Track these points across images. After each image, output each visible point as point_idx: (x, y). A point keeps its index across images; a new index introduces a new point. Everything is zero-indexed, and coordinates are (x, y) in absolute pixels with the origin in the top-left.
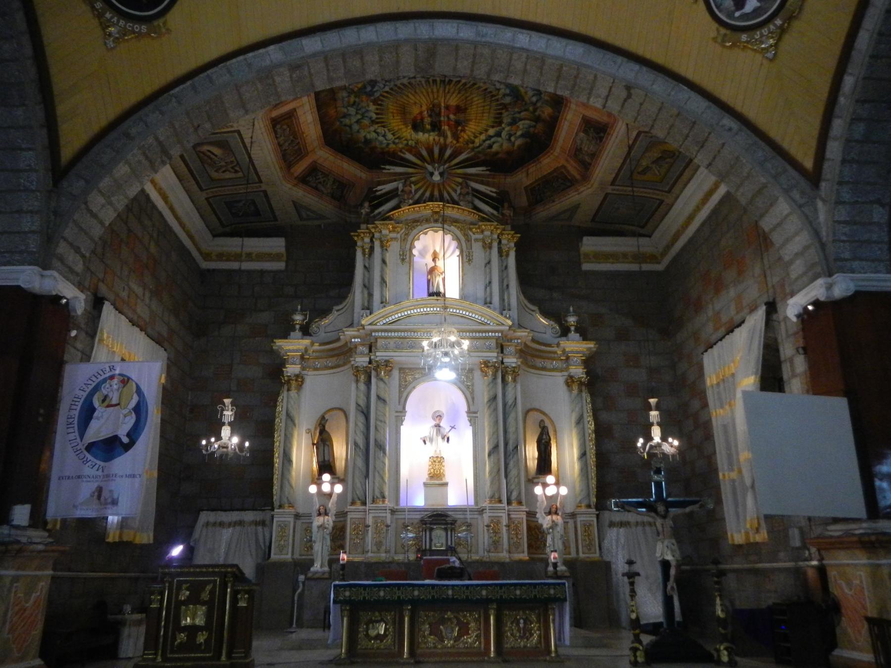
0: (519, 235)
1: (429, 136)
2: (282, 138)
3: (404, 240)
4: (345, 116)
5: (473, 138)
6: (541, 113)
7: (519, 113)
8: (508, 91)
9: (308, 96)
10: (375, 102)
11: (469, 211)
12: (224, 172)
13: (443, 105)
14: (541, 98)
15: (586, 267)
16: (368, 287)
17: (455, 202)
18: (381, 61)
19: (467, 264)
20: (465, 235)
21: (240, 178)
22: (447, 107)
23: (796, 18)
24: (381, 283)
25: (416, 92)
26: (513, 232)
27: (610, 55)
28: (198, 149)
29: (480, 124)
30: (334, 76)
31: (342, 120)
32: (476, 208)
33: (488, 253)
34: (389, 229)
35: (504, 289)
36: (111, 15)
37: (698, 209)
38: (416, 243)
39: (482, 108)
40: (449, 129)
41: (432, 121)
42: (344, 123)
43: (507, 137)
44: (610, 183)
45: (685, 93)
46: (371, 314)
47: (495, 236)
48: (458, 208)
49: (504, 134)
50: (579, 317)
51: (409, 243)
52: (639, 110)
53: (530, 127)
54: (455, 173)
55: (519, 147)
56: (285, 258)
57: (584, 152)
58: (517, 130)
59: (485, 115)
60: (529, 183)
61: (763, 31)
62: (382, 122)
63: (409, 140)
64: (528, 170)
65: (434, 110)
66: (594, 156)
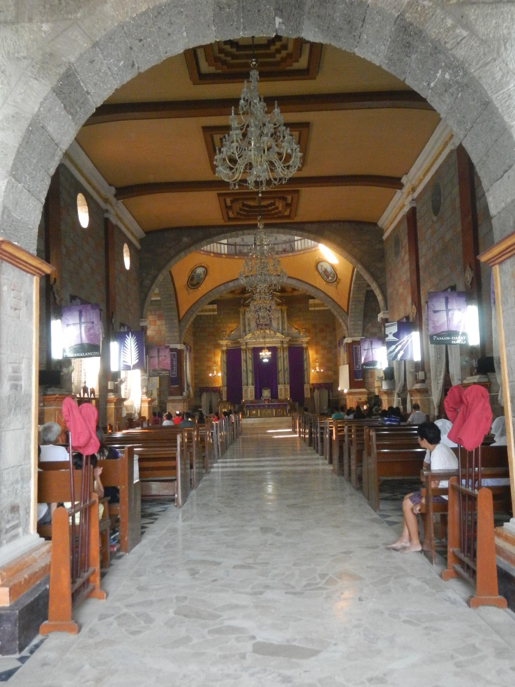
15: (310, 309)
16: (244, 325)
35: (283, 324)
46: (246, 335)
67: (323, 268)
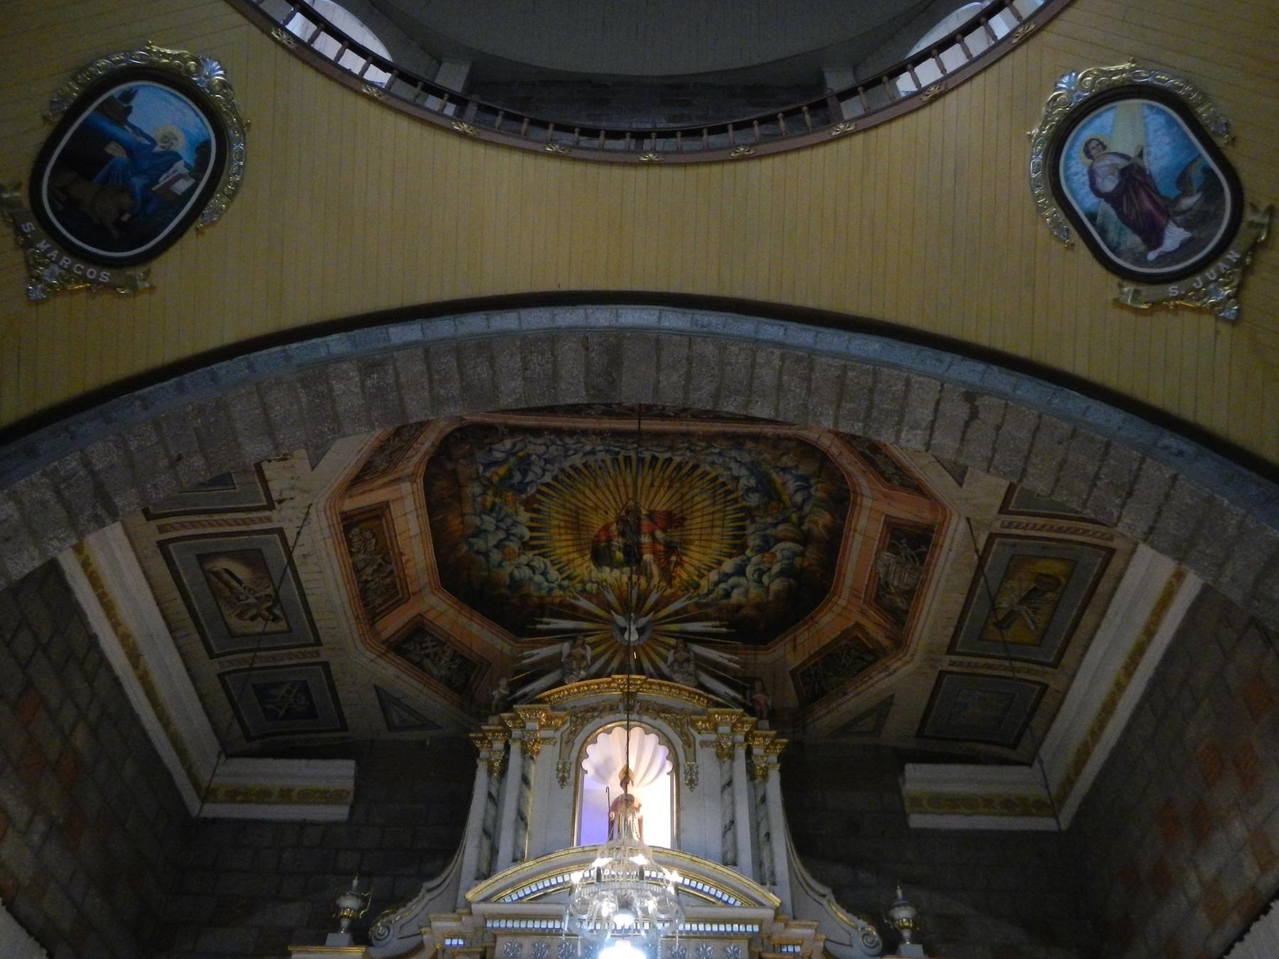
0: (785, 741)
1: (622, 573)
2: (361, 556)
3: (566, 743)
4: (480, 532)
5: (696, 579)
6: (813, 526)
7: (775, 525)
8: (753, 482)
9: (412, 483)
10: (529, 505)
11: (690, 692)
12: (253, 618)
13: (644, 512)
14: (809, 493)
16: (491, 834)
17: (662, 676)
18: (526, 369)
19: (685, 790)
20: (683, 734)
21: (282, 632)
22: (651, 515)
23: (1264, 245)
24: (516, 821)
25: (597, 485)
26: (773, 733)
27: (928, 352)
28: (208, 566)
29: (708, 551)
30: (442, 392)
31: (474, 540)
32: (701, 686)
33: (726, 766)
34: (540, 720)
35: (761, 839)
36: (48, 246)
37: (1120, 687)
38: (590, 749)
39: (710, 517)
40: (655, 561)
41: (626, 545)
42: (476, 548)
43: (756, 576)
44: (945, 649)
45: (1076, 402)
47: (740, 738)
48: (671, 687)
49: (749, 570)
50: (917, 907)
51: (577, 748)
52: (995, 442)
53: (795, 554)
54: (663, 642)
55: (778, 594)
56: (350, 799)
57: (893, 590)
58: (772, 563)
59: (718, 530)
60: (799, 662)
61: (1207, 274)
62: (542, 546)
63: (587, 582)
64: (795, 639)
65: (630, 523)
66: (911, 594)
67: (1103, 166)
